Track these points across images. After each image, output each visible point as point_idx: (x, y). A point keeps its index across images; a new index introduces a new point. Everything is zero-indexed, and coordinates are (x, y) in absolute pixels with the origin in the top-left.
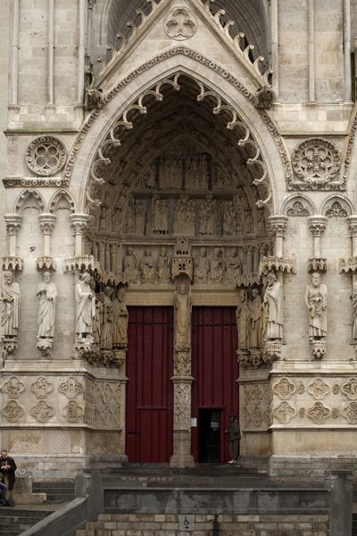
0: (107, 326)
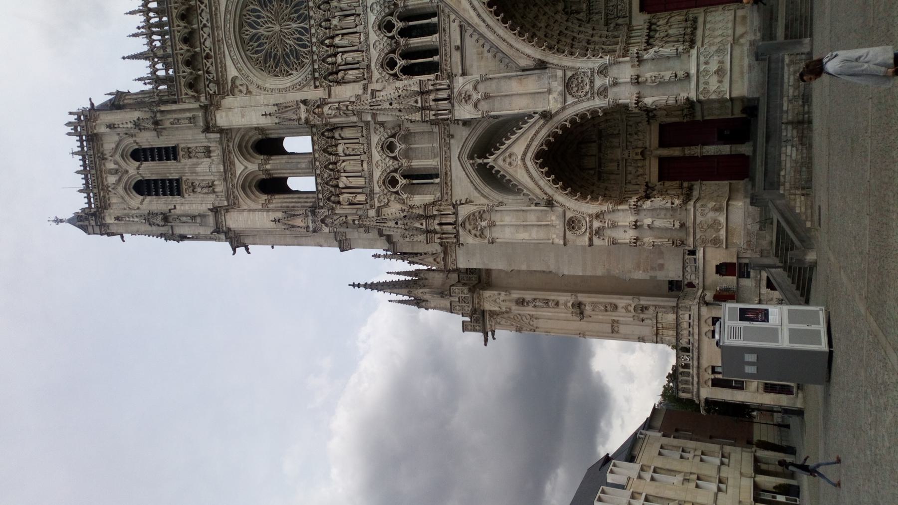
0: (669, 192)
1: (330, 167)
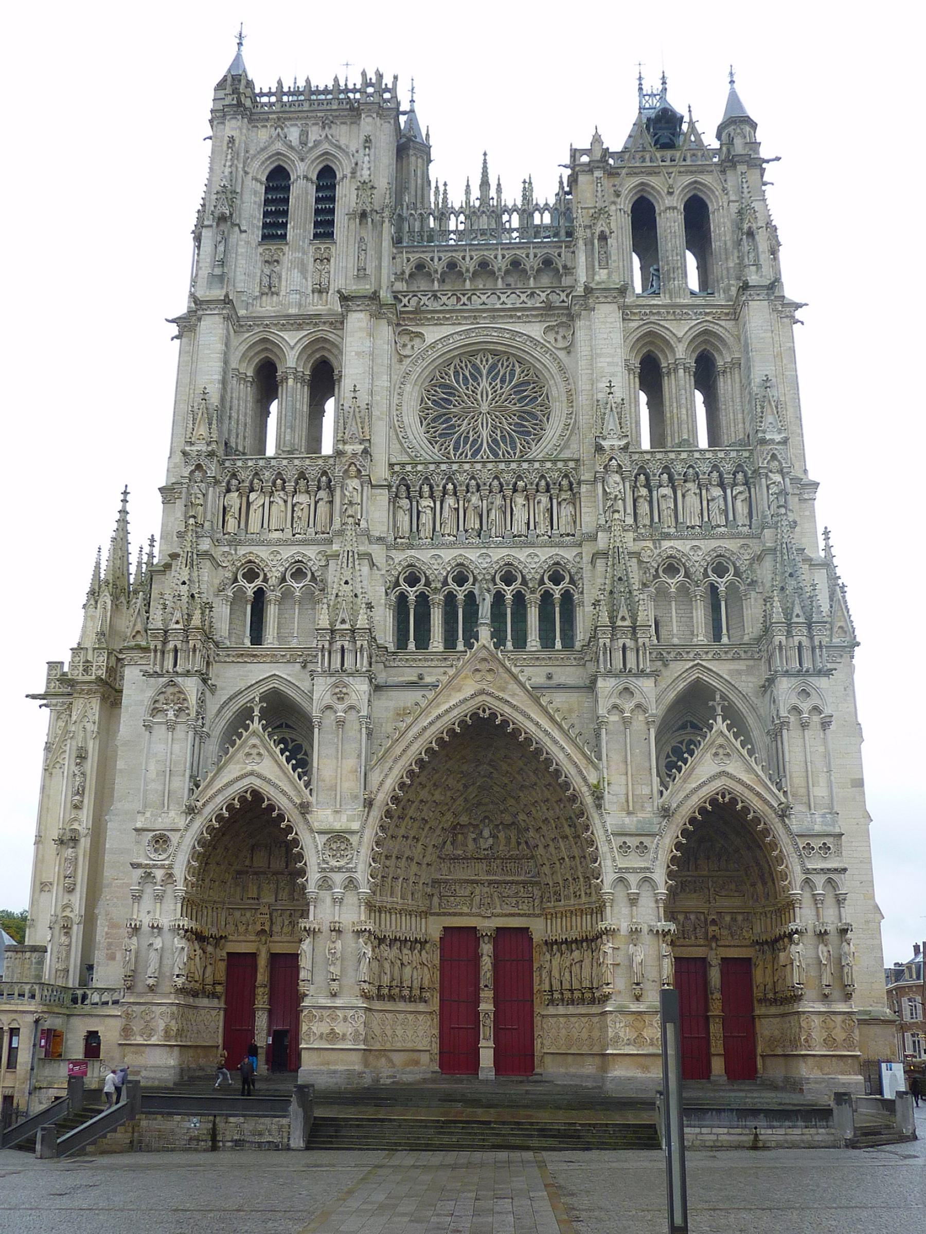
1: (279, 481)
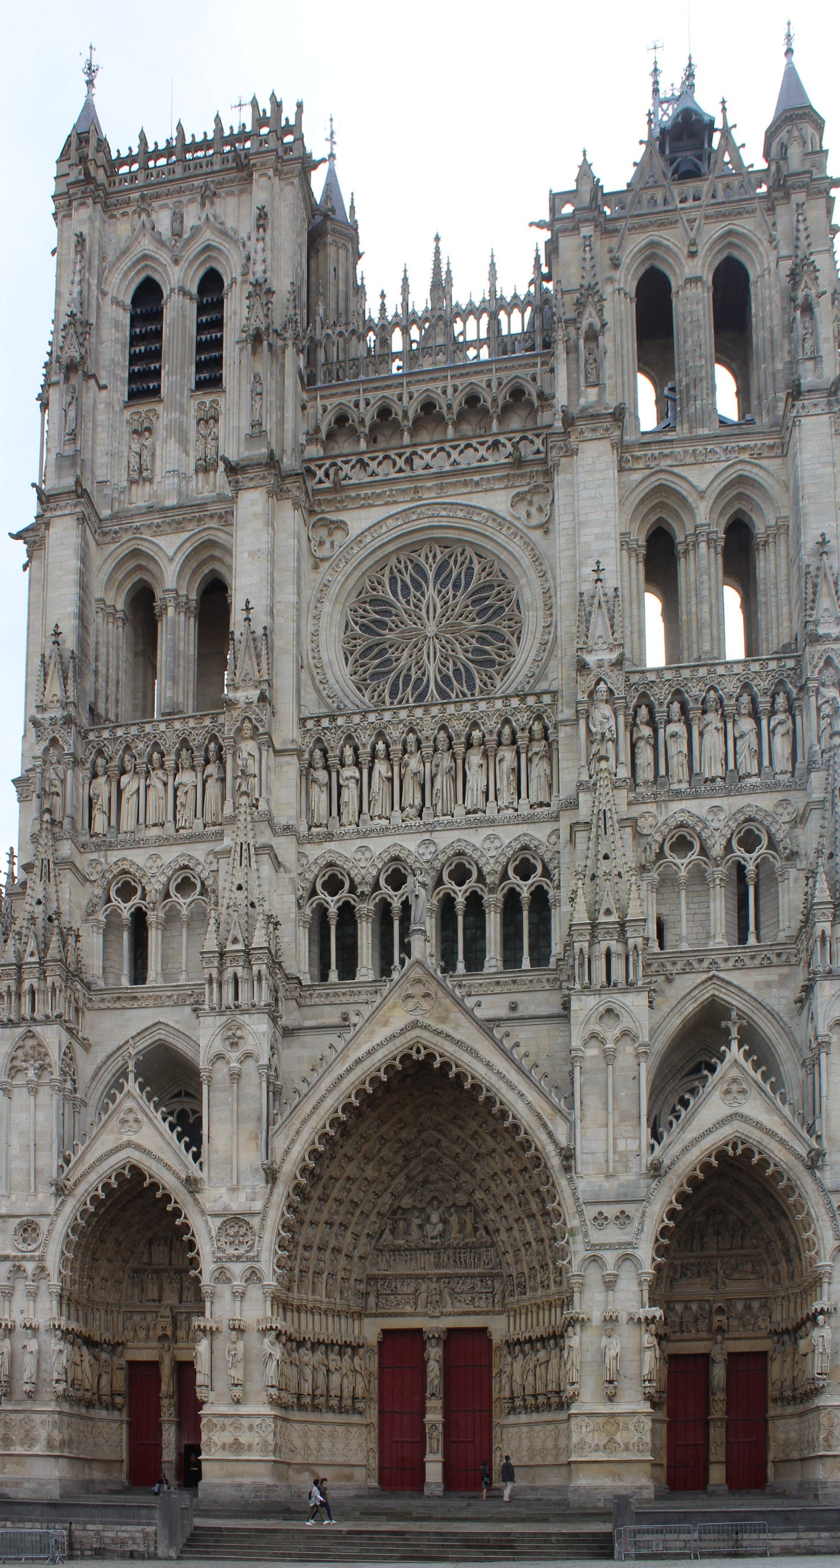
1: (156, 756)
